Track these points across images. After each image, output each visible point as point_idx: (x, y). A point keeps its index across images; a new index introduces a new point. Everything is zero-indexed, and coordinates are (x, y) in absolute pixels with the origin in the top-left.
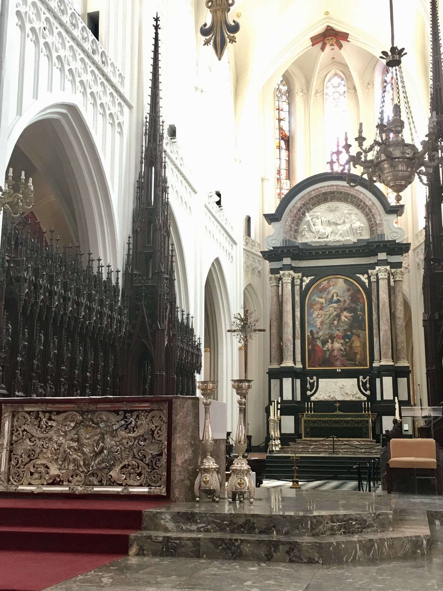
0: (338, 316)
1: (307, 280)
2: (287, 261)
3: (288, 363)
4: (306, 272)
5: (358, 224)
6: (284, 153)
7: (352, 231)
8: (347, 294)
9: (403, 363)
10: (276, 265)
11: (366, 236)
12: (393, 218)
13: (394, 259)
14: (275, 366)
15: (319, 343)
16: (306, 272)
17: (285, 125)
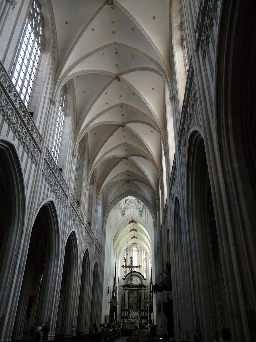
0: (135, 299)
1: (129, 292)
2: (126, 288)
3: (126, 309)
4: (129, 290)
5: (139, 281)
6: (125, 262)
7: (138, 283)
8: (137, 295)
9: (146, 309)
10: (124, 288)
11: (140, 284)
12: (145, 281)
13: (145, 288)
14: (123, 309)
15: (131, 304)
16: (129, 290)
17: (125, 257)
